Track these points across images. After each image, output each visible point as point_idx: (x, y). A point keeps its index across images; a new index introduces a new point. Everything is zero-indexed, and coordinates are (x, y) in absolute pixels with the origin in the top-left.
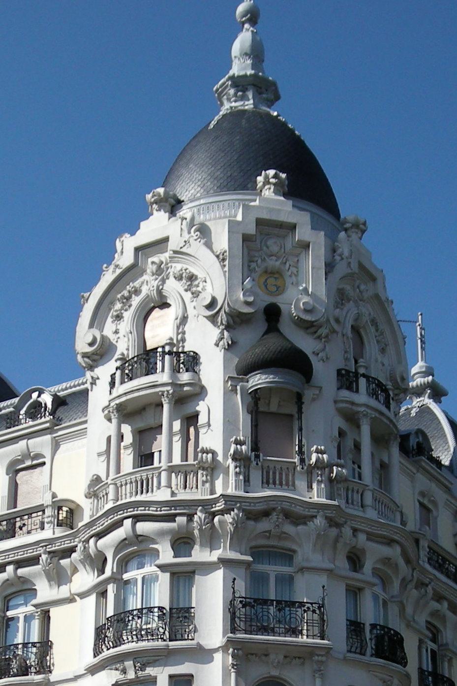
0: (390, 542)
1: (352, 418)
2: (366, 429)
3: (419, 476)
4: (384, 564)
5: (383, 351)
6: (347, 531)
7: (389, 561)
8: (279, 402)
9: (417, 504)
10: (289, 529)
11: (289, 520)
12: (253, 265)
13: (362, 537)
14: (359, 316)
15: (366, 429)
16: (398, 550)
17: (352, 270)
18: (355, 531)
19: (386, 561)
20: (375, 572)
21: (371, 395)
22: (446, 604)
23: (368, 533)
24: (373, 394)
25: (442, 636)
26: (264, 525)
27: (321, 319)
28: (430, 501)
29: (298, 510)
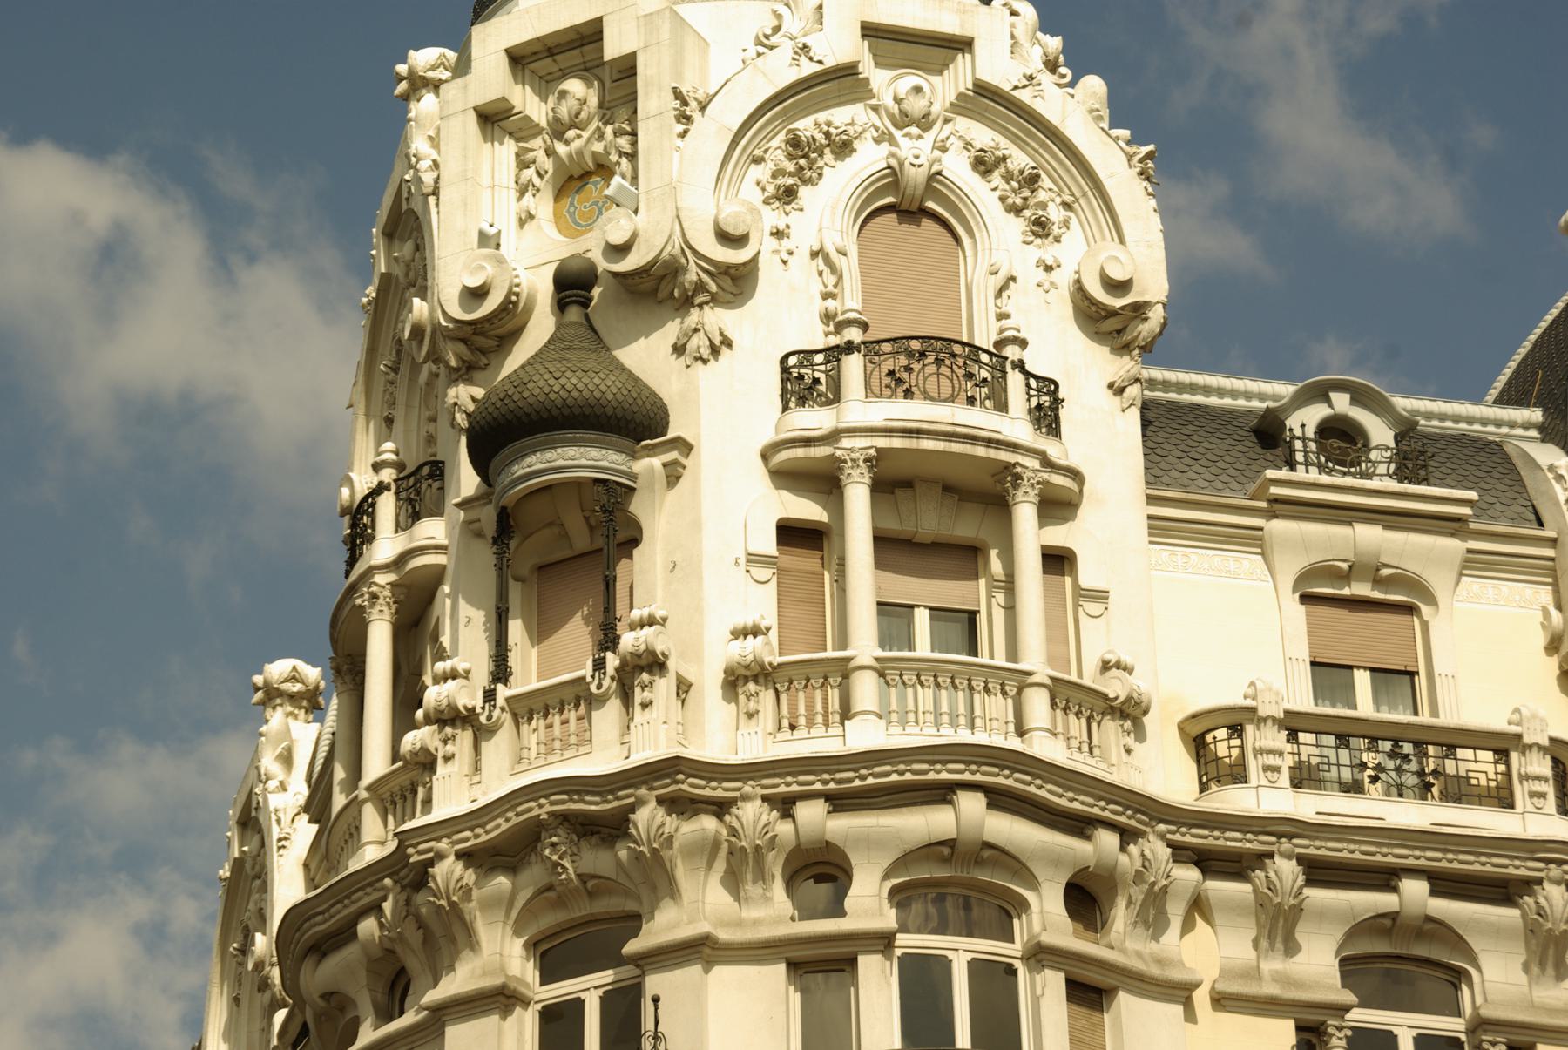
0: (942, 794)
1: (823, 481)
2: (858, 496)
3: (1277, 527)
4: (946, 861)
5: (1041, 228)
6: (752, 814)
7: (952, 848)
8: (587, 519)
9: (1298, 612)
10: (596, 860)
11: (594, 840)
12: (530, 173)
13: (811, 814)
14: (894, 173)
15: (858, 496)
16: (972, 805)
17: (820, 62)
18: (785, 805)
19: (944, 849)
20: (900, 896)
21: (887, 392)
22: (1415, 890)
23: (829, 797)
24: (897, 384)
25: (1471, 986)
26: (533, 876)
27: (665, 254)
28: (1378, 582)
29: (593, 805)
